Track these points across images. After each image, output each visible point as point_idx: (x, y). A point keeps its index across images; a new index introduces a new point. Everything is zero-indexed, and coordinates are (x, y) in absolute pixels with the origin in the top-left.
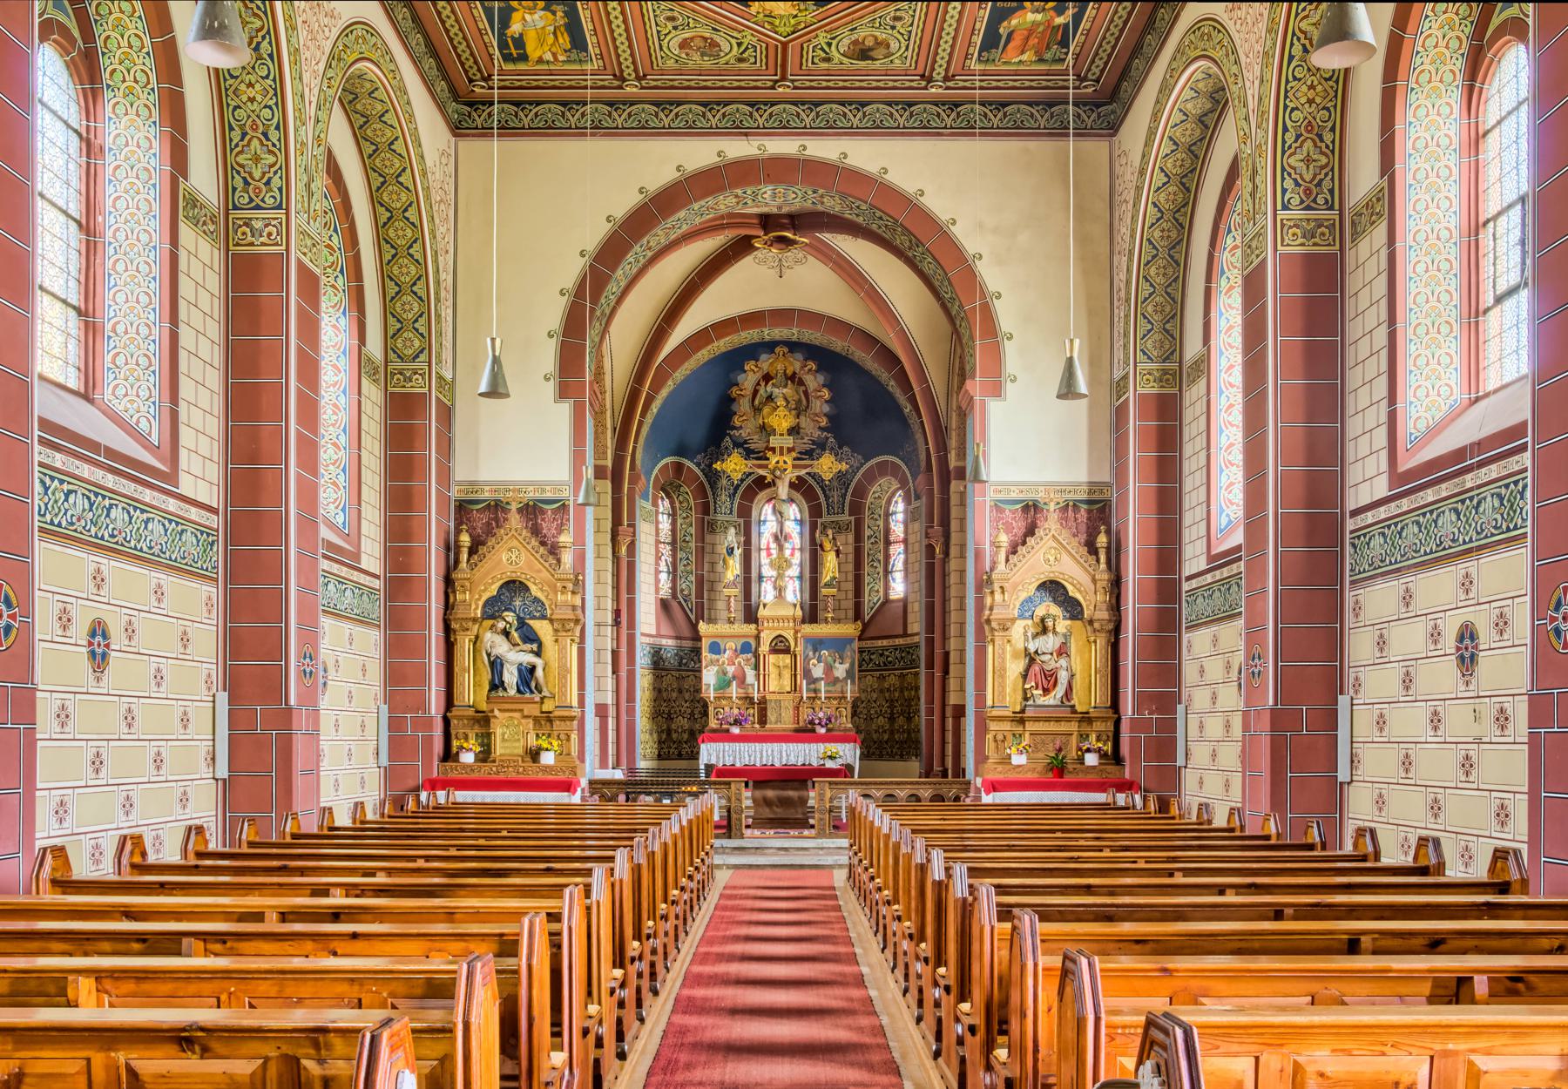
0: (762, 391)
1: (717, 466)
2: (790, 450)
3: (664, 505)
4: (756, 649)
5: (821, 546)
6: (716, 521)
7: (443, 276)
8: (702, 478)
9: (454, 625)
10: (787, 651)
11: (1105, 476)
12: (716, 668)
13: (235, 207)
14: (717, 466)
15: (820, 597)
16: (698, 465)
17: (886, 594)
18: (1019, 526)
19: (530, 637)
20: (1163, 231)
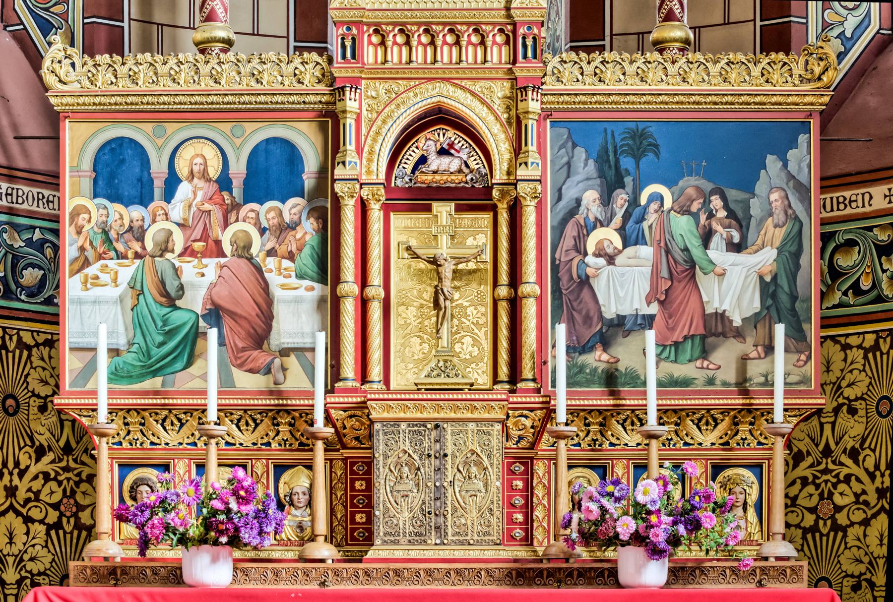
12: (127, 271)
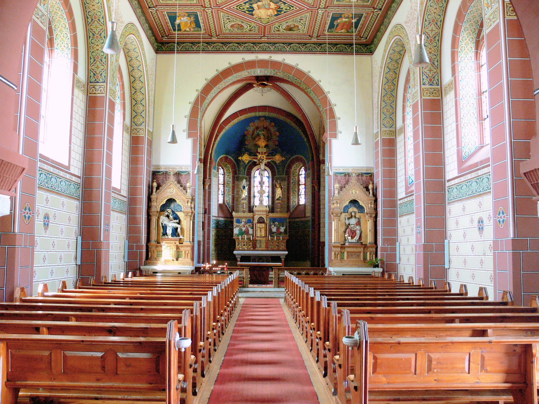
0: (255, 133)
1: (240, 158)
2: (265, 153)
3: (221, 171)
4: (253, 222)
5: (276, 186)
6: (239, 177)
7: (151, 98)
8: (235, 162)
9: (151, 214)
10: (263, 222)
11: (372, 165)
13: (91, 82)
14: (240, 158)
15: (275, 204)
16: (233, 157)
17: (298, 203)
18: (343, 182)
19: (176, 218)
20: (389, 86)
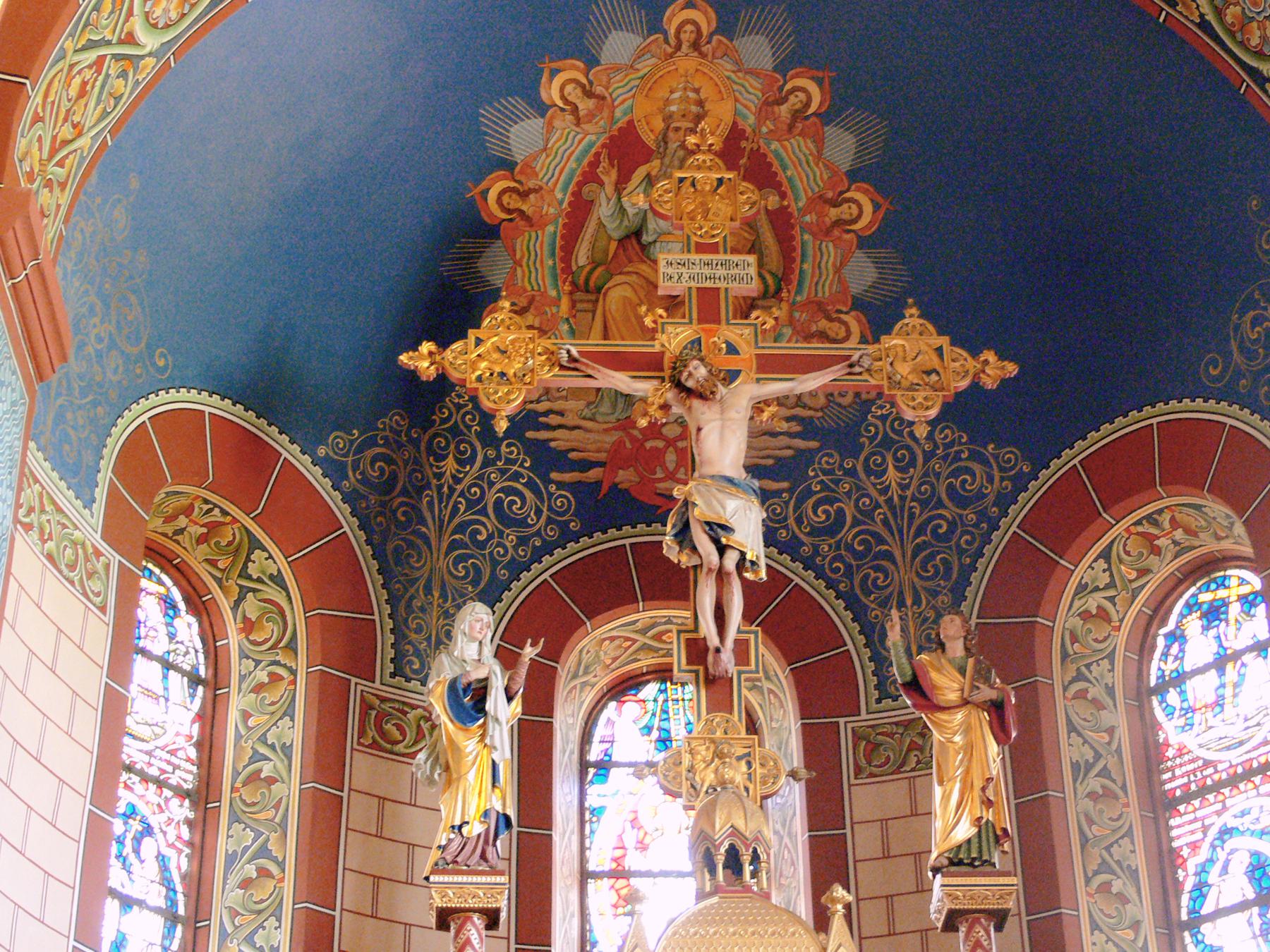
0: (604, 210)
16: (335, 471)
